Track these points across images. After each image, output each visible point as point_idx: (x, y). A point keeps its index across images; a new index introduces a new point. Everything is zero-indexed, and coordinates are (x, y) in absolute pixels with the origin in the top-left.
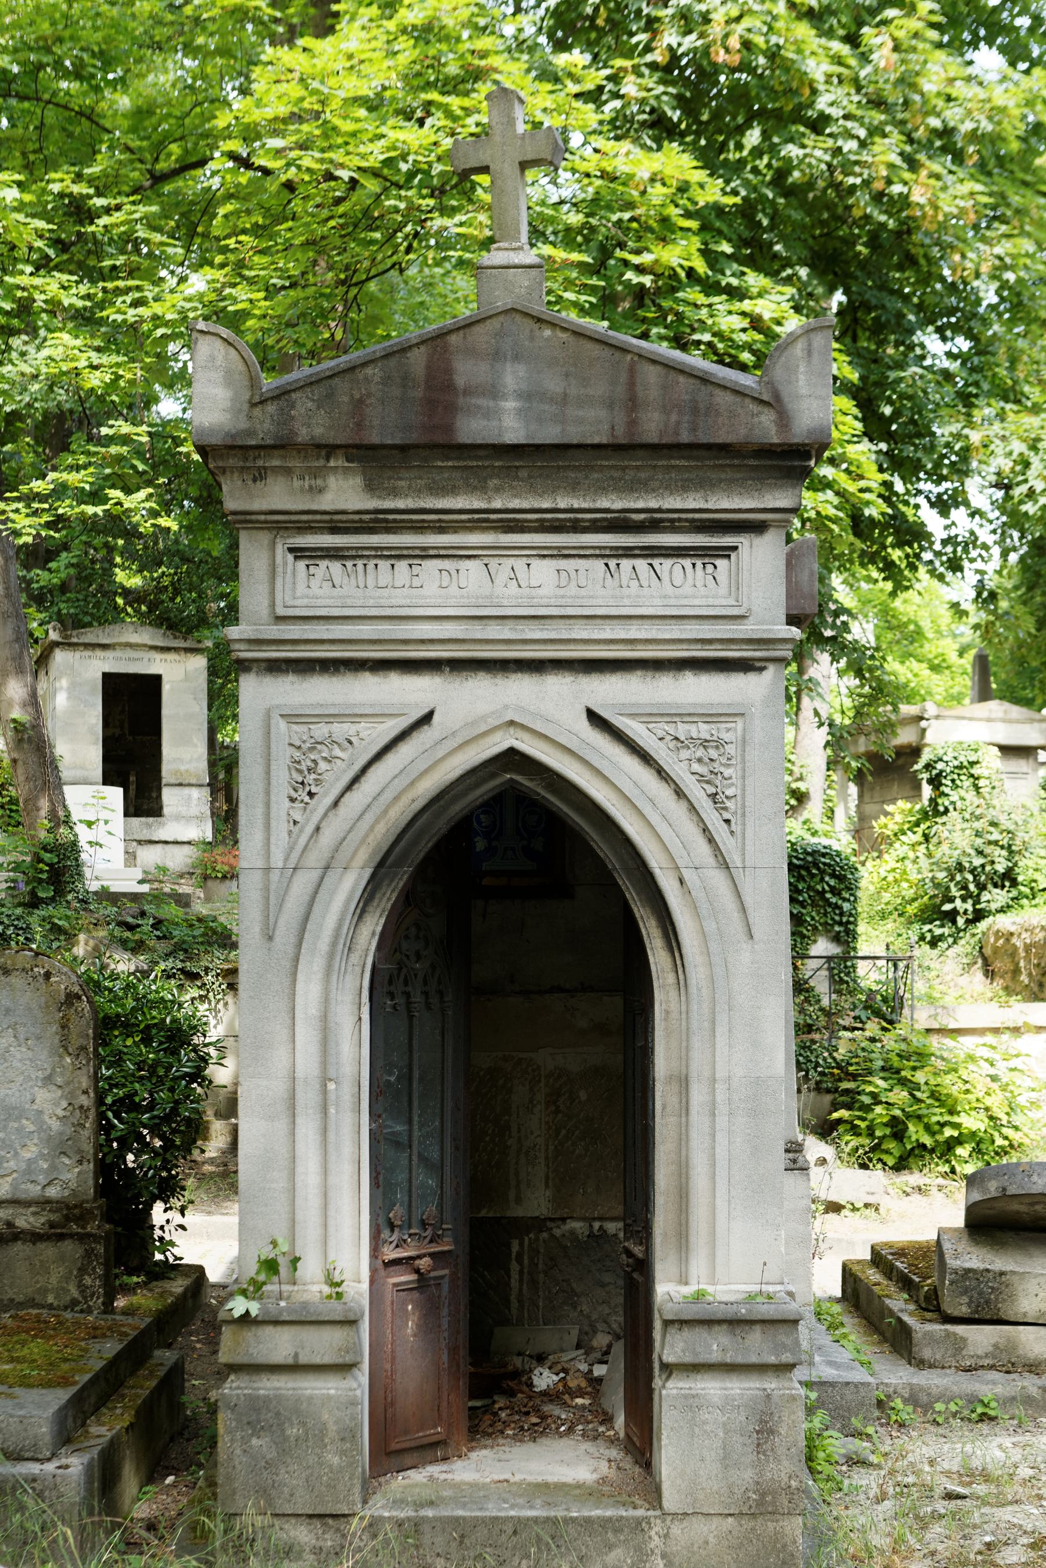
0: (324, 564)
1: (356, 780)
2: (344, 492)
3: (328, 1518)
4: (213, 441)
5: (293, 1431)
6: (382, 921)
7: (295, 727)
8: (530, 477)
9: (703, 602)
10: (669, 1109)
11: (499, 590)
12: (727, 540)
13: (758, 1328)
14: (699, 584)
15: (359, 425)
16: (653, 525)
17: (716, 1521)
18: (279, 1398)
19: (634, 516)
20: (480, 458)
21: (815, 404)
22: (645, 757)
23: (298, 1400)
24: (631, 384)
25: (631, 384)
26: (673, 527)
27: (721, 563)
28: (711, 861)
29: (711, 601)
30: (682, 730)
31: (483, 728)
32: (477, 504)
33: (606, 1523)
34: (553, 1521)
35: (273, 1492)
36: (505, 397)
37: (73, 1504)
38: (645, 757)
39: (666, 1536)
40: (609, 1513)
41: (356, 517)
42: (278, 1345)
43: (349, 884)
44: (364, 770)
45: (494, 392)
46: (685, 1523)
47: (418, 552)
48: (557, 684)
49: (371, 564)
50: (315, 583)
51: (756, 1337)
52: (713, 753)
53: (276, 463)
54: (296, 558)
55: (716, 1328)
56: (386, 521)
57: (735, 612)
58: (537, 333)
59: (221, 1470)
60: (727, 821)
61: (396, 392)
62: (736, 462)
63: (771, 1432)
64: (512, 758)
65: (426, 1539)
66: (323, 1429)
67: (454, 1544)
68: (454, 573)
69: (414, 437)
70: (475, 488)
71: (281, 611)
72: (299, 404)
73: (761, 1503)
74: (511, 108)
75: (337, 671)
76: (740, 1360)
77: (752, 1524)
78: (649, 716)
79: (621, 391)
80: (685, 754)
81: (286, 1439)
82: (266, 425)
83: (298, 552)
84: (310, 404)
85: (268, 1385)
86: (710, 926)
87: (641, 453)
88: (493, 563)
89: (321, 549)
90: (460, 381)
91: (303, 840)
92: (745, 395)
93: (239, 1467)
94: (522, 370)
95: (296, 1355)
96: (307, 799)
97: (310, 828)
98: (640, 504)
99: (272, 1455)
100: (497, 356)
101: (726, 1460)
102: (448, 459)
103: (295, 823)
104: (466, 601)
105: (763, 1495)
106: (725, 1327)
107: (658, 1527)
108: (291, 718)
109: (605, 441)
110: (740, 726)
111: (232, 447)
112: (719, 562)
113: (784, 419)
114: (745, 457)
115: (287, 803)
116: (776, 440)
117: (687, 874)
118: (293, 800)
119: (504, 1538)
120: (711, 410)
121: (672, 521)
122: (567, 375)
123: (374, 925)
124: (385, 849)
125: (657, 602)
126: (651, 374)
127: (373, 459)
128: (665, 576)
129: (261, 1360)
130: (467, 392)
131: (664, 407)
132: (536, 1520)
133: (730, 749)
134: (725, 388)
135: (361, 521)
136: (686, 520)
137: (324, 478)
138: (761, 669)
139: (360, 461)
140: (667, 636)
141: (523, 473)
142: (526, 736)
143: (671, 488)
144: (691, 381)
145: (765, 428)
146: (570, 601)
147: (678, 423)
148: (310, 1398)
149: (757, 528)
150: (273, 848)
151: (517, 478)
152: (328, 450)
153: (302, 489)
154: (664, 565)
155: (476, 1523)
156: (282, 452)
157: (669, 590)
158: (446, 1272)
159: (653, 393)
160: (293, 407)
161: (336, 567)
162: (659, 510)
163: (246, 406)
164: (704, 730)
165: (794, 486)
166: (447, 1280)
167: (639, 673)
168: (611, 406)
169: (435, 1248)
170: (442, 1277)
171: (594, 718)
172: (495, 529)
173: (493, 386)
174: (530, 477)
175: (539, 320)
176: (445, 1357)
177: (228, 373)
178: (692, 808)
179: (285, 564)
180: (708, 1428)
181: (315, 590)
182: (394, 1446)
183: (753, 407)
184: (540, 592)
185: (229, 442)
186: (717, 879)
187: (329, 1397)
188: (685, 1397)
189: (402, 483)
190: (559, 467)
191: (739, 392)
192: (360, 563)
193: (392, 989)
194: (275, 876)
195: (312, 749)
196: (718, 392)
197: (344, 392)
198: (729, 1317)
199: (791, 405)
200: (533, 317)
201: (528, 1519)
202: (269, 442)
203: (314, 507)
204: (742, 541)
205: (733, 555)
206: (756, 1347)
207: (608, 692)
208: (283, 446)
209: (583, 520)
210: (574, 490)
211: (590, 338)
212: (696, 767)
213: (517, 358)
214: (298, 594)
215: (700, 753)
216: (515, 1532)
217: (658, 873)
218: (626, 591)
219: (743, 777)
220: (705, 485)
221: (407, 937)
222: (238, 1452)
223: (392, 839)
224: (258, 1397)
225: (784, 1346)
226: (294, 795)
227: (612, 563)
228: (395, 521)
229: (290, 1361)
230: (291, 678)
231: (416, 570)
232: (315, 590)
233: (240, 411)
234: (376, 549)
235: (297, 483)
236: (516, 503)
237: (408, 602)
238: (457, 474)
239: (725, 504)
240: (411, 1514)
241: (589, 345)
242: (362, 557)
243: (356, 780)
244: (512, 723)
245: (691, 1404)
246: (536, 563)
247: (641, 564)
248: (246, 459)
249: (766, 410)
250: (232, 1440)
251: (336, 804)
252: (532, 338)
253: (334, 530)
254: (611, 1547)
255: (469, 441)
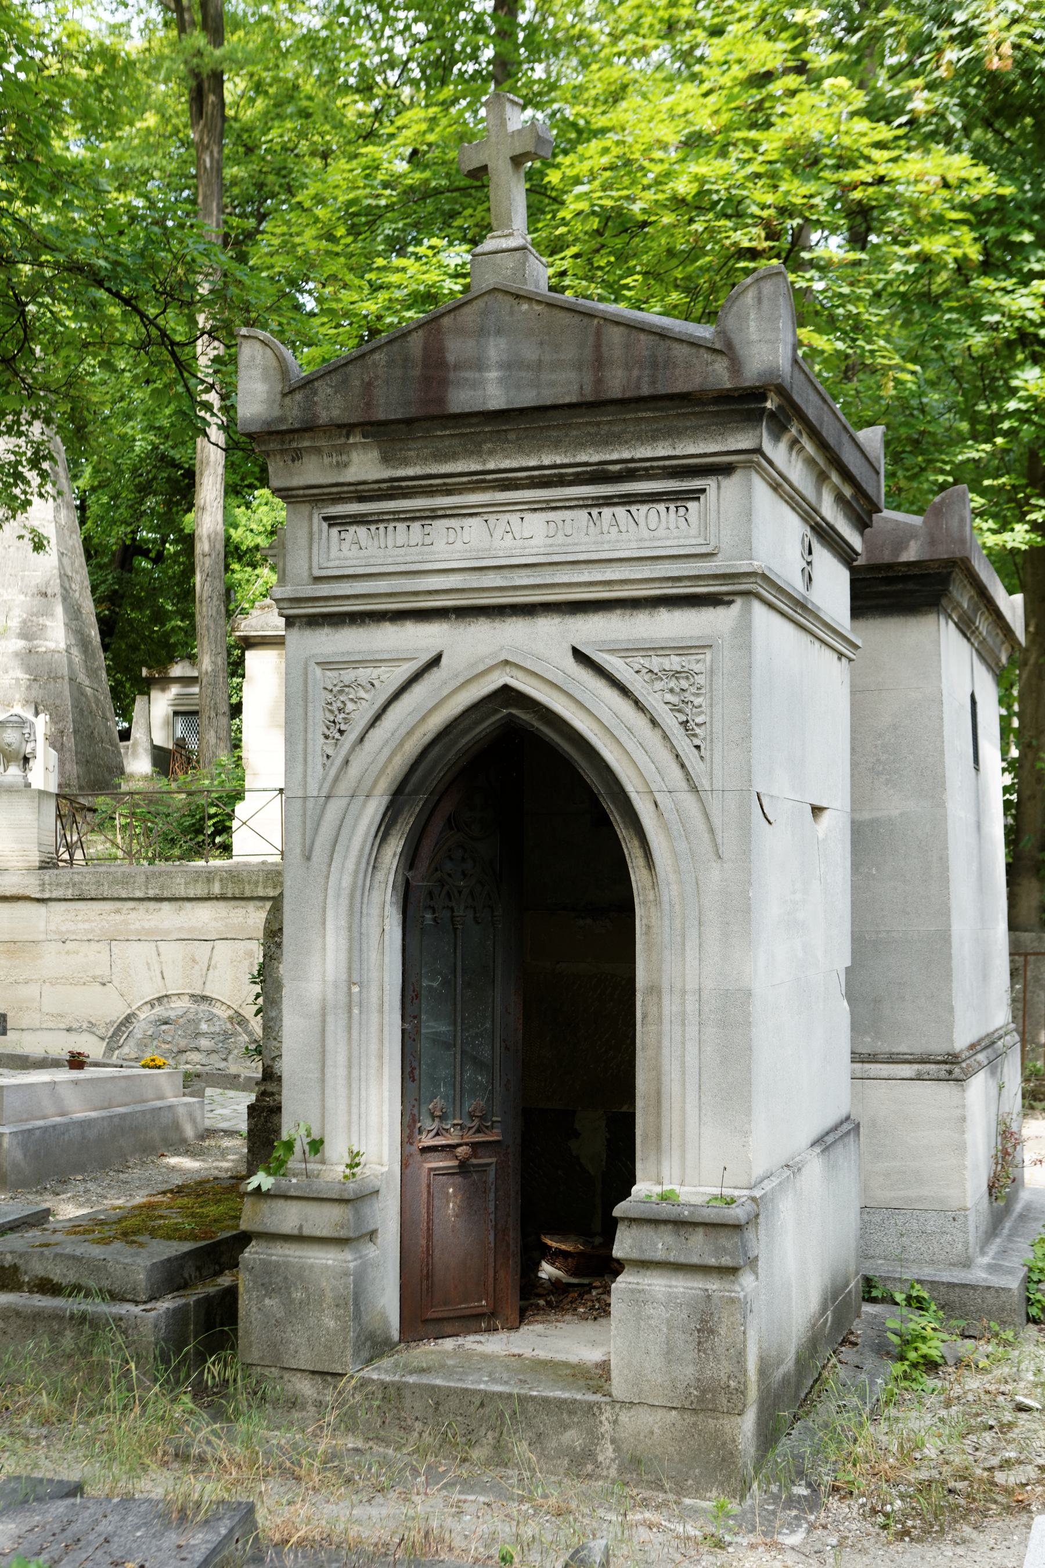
0: (352, 529)
1: (377, 718)
2: (364, 465)
3: (326, 1376)
4: (253, 429)
5: (297, 1295)
6: (402, 842)
7: (328, 673)
8: (518, 439)
9: (675, 542)
10: (650, 1018)
11: (497, 543)
12: (696, 483)
13: (701, 1230)
14: (672, 526)
15: (368, 405)
16: (630, 474)
17: (661, 1413)
18: (287, 1264)
19: (611, 467)
20: (471, 425)
21: (764, 348)
22: (624, 690)
23: (302, 1268)
24: (598, 346)
25: (598, 346)
26: (648, 474)
27: (692, 505)
28: (683, 785)
29: (682, 542)
30: (656, 663)
31: (482, 668)
32: (475, 467)
33: (561, 1403)
34: (523, 1399)
35: (282, 1348)
36: (488, 369)
37: (149, 1343)
38: (624, 690)
39: (615, 1422)
40: (566, 1395)
41: (376, 486)
42: (289, 1217)
43: (374, 809)
44: (385, 708)
45: (479, 365)
46: (632, 1412)
47: (428, 514)
48: (547, 626)
49: (391, 525)
50: (345, 546)
51: (698, 1239)
52: (684, 684)
53: (306, 444)
54: (330, 525)
55: (662, 1228)
56: (401, 487)
57: (704, 550)
58: (516, 308)
59: (241, 1324)
60: (698, 747)
61: (398, 372)
62: (697, 409)
63: (712, 1331)
64: (506, 694)
65: (407, 1402)
66: (322, 1293)
67: (431, 1410)
68: (459, 530)
69: (413, 412)
70: (472, 453)
71: (317, 573)
72: (320, 390)
73: (701, 1399)
74: (503, 110)
75: (363, 622)
76: (682, 1259)
77: (694, 1419)
78: (626, 651)
79: (588, 353)
80: (658, 685)
81: (292, 1301)
82: (295, 412)
83: (331, 521)
84: (329, 390)
85: (280, 1252)
86: (682, 846)
87: (611, 408)
88: (492, 518)
89: (349, 516)
90: (451, 358)
91: (333, 772)
92: (700, 346)
93: (255, 1323)
94: (503, 342)
95: (301, 1227)
96: (337, 735)
97: (339, 761)
98: (615, 456)
99: (280, 1314)
100: (482, 332)
101: (669, 1353)
102: (446, 428)
103: (328, 757)
104: (468, 555)
105: (704, 1392)
106: (670, 1227)
107: (607, 1414)
108: (325, 665)
109: (574, 400)
110: (708, 657)
111: (270, 433)
112: (690, 505)
113: (735, 365)
114: (704, 404)
115: (322, 740)
116: (728, 386)
117: (659, 797)
118: (327, 737)
119: (472, 1409)
120: (669, 363)
121: (646, 469)
122: (541, 343)
123: (395, 846)
124: (399, 779)
125: (634, 545)
126: (616, 335)
127: (387, 433)
128: (641, 521)
129: (272, 1229)
130: (457, 367)
131: (627, 364)
132: (500, 1395)
133: (700, 680)
134: (682, 341)
135: (380, 489)
136: (658, 467)
137: (348, 453)
138: (730, 603)
139: (373, 437)
140: (639, 576)
141: (512, 436)
142: (520, 674)
143: (642, 439)
144: (652, 337)
145: (719, 375)
146: (556, 549)
147: (639, 378)
148: (312, 1266)
149: (725, 470)
150: (309, 779)
151: (507, 440)
152: (347, 428)
153: (331, 464)
154: (641, 511)
155: (450, 1392)
156: (311, 434)
157: (646, 534)
158: (493, 1160)
159: (618, 353)
160: (315, 394)
161: (361, 531)
162: (632, 460)
163: (279, 397)
164: (674, 662)
165: (754, 428)
166: (493, 1167)
167: (619, 612)
168: (580, 369)
169: (480, 1138)
170: (489, 1165)
171: (579, 655)
172: (493, 488)
173: (479, 359)
174: (518, 439)
175: (518, 296)
176: (491, 1238)
177: (265, 369)
178: (665, 737)
179: (321, 531)
180: (652, 1322)
181: (345, 552)
182: (430, 1315)
183: (707, 356)
184: (532, 542)
185: (266, 429)
186: (688, 800)
187: (327, 1267)
188: (632, 1291)
189: (411, 453)
190: (541, 428)
191: (694, 344)
192: (381, 526)
193: (421, 905)
194: (310, 803)
195: (341, 692)
196: (676, 346)
197: (356, 377)
198: (672, 1217)
199: (742, 351)
200: (512, 294)
201: (494, 1393)
202: (297, 426)
203: (341, 480)
204: (710, 483)
205: (702, 497)
206: (698, 1248)
207: (592, 631)
208: (309, 428)
209: (567, 474)
210: (556, 447)
211: (562, 308)
212: (669, 697)
213: (499, 332)
214: (332, 556)
215: (673, 684)
216: (482, 1405)
217: (634, 796)
218: (607, 537)
219: (711, 705)
220: (673, 434)
221: (451, 859)
222: (254, 1309)
223: (406, 769)
224: (270, 1262)
225: (724, 1249)
226: (328, 733)
227: (595, 512)
228: (408, 487)
229: (296, 1232)
230: (327, 630)
231: (427, 529)
232: (345, 552)
233: (274, 401)
234: (394, 513)
235: (327, 460)
236: (506, 464)
237: (419, 558)
238: (455, 442)
239: (692, 450)
240: (397, 1378)
241: (562, 314)
242: (383, 521)
243: (377, 718)
244: (506, 662)
245: (638, 1298)
246: (528, 516)
247: (620, 511)
248: (283, 442)
249: (719, 358)
250: (250, 1299)
251: (362, 739)
252: (512, 313)
253: (361, 499)
254: (566, 1427)
255: (459, 411)
